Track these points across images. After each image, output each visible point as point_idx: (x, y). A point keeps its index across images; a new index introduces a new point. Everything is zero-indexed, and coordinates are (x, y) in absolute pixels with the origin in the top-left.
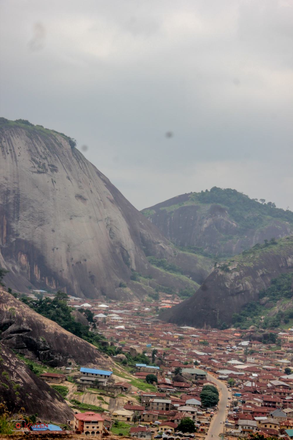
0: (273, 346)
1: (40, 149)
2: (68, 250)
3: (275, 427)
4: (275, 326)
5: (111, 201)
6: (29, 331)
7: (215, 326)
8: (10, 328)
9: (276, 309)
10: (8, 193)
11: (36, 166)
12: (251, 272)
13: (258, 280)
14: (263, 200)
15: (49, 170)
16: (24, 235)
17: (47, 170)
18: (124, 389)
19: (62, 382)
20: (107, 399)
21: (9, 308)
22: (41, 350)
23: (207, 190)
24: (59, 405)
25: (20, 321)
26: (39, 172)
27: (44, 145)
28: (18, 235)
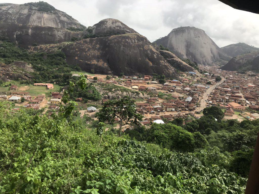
1: (197, 33)
2: (201, 54)
4: (246, 71)
9: (247, 67)
10: (188, 42)
12: (242, 59)
13: (244, 61)
16: (191, 51)
20: (193, 78)
24: (180, 77)
25: (177, 62)
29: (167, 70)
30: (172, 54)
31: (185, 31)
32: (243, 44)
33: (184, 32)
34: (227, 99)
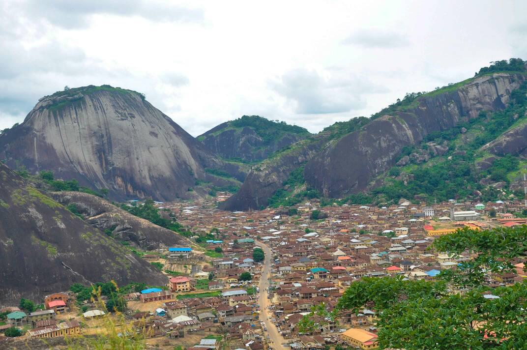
0: (296, 216)
1: (121, 104)
2: (150, 170)
3: (304, 268)
5: (174, 133)
6: (130, 228)
7: (256, 208)
8: (117, 229)
11: (120, 115)
12: (275, 170)
14: (277, 121)
15: (129, 117)
17: (127, 117)
18: (201, 259)
19: (158, 260)
21: (114, 214)
22: (140, 240)
23: (239, 118)
25: (123, 222)
26: (123, 120)
27: (123, 100)
28: (113, 165)
29: (114, 260)
30: (97, 198)
31: (84, 103)
32: (256, 118)
33: (80, 106)
34: (330, 323)
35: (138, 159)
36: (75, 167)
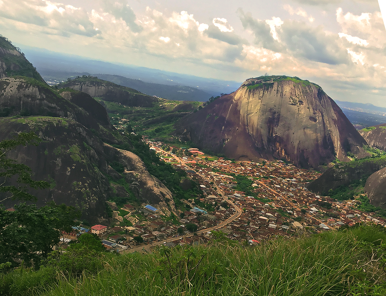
6: (138, 185)
10: (275, 113)
11: (292, 101)
26: (292, 104)
35: (293, 134)
36: (248, 129)
